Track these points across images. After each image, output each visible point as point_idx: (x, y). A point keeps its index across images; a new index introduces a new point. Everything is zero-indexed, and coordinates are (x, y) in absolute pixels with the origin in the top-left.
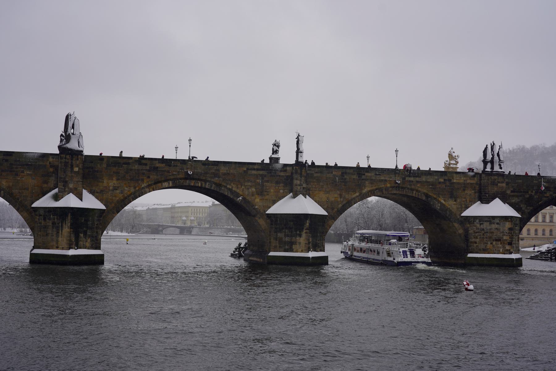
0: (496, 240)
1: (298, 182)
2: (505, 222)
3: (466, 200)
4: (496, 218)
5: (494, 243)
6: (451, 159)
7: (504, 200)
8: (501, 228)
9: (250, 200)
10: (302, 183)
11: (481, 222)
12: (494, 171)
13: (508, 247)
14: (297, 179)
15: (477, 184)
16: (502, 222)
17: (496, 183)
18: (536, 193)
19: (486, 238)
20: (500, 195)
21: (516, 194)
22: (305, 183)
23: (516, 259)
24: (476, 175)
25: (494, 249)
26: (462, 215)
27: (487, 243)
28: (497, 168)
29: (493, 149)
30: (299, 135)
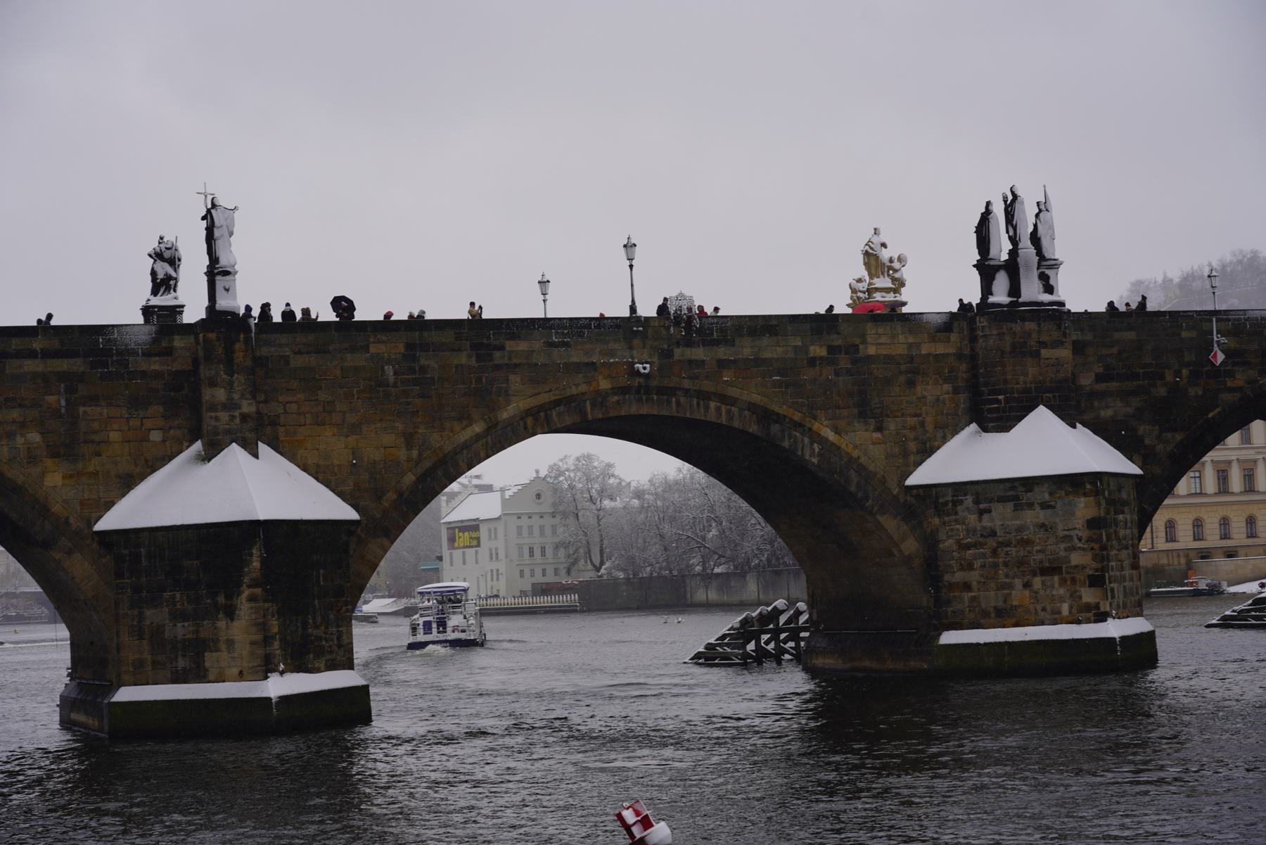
1: (221, 395)
3: (922, 424)
4: (1037, 484)
5: (1037, 582)
6: (873, 272)
7: (1070, 416)
8: (1057, 520)
9: (20, 480)
10: (236, 396)
11: (982, 506)
12: (1020, 300)
14: (213, 383)
15: (959, 356)
16: (1060, 498)
19: (1006, 564)
20: (1051, 395)
21: (1114, 385)
22: (248, 396)
23: (1123, 638)
24: (956, 324)
25: (1039, 607)
26: (912, 480)
27: (1011, 586)
28: (1031, 291)
30: (214, 206)
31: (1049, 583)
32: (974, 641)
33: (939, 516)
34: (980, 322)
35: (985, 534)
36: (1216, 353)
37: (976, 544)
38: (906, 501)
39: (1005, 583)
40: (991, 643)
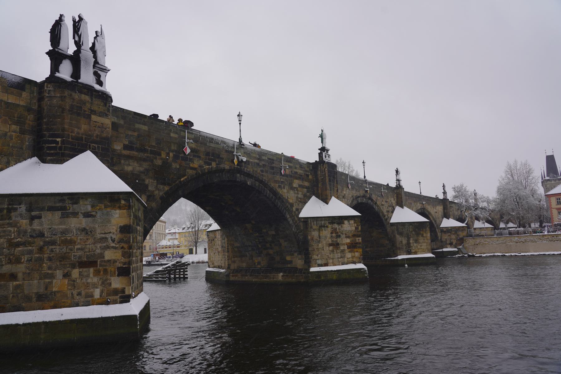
0: (83, 264)
2: (108, 210)
4: (82, 198)
5: (75, 273)
8: (97, 226)
11: (33, 213)
13: (117, 283)
15: (29, 109)
17: (85, 111)
18: (176, 157)
19: (50, 259)
20: (96, 146)
21: (135, 153)
25: (75, 292)
27: (52, 276)
29: (79, 29)
31: (85, 274)
32: (14, 322)
34: (47, 87)
35: (35, 235)
36: (186, 148)
37: (25, 242)
39: (48, 273)
40: (29, 324)
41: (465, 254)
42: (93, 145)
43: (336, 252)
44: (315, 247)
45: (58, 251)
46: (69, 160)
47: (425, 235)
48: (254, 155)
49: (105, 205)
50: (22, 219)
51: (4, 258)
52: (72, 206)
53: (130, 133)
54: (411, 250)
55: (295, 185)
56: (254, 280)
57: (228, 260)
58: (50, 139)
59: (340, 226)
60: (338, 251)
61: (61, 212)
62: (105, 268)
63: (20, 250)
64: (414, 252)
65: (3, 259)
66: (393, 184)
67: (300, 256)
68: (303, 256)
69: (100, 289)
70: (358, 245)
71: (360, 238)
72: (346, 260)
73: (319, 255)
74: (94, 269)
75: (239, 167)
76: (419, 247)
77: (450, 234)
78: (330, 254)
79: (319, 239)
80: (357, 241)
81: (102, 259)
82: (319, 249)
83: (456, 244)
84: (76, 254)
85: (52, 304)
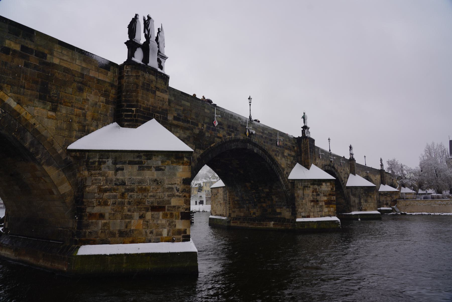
0: (154, 209)
2: (174, 165)
3: (85, 115)
4: (155, 155)
5: (149, 215)
8: (165, 178)
11: (118, 166)
13: (180, 225)
15: (112, 85)
17: (152, 88)
18: (208, 128)
19: (129, 203)
20: (159, 115)
21: (181, 123)
25: (148, 231)
27: (131, 217)
31: (156, 216)
32: (103, 253)
33: (88, 170)
34: (126, 68)
35: (118, 183)
36: (215, 121)
37: (111, 189)
38: (67, 159)
39: (128, 214)
40: (114, 255)
41: (398, 212)
42: (157, 114)
43: (316, 207)
44: (300, 203)
45: (136, 197)
46: (141, 125)
47: (372, 197)
48: (260, 130)
49: (171, 161)
50: (109, 170)
51: (95, 201)
52: (147, 161)
53: (178, 107)
54: (361, 208)
55: (286, 154)
56: (250, 226)
57: (229, 210)
58: (127, 108)
59: (319, 187)
60: (317, 206)
61: (139, 166)
62: (171, 212)
63: (107, 195)
64: (364, 210)
65: (94, 202)
66: (348, 157)
67: (288, 209)
68: (291, 209)
69: (168, 230)
70: (333, 202)
71: (335, 197)
72: (324, 214)
73: (303, 209)
74: (162, 213)
75: (249, 138)
76: (368, 206)
77: (386, 196)
78: (312, 208)
79: (303, 196)
80: (332, 199)
81: (169, 205)
82: (303, 204)
83: (391, 204)
84: (149, 201)
85: (131, 240)
